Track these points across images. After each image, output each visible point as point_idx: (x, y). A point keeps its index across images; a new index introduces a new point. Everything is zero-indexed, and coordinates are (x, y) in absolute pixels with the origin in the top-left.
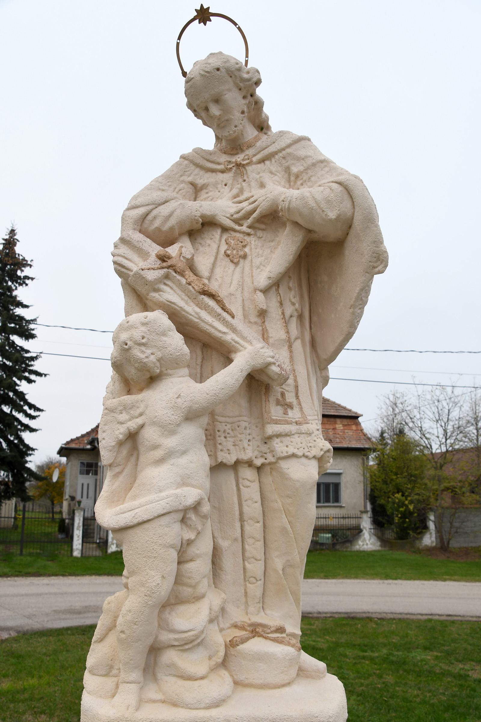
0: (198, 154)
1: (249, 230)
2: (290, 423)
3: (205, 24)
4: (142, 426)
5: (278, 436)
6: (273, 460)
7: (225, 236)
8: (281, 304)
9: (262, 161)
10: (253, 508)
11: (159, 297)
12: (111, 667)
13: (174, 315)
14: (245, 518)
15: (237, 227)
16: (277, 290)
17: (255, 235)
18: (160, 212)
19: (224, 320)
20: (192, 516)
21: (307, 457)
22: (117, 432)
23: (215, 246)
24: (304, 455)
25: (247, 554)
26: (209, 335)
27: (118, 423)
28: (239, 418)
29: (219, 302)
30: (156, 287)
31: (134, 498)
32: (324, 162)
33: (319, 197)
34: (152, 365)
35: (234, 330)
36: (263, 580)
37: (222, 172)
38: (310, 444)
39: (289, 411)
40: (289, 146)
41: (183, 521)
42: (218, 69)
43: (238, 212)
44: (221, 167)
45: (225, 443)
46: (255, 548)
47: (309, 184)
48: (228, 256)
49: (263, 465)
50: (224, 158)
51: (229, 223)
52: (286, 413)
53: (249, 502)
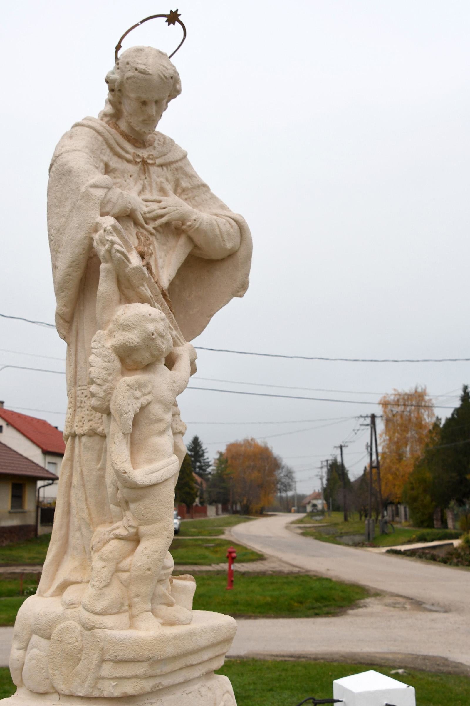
0: (111, 135)
1: (154, 231)
3: (169, 25)
4: (149, 403)
9: (161, 166)
12: (122, 604)
18: (111, 198)
19: (172, 318)
22: (135, 406)
27: (135, 398)
31: (150, 461)
32: (204, 186)
33: (223, 229)
37: (128, 161)
43: (149, 212)
47: (193, 202)
50: (128, 146)
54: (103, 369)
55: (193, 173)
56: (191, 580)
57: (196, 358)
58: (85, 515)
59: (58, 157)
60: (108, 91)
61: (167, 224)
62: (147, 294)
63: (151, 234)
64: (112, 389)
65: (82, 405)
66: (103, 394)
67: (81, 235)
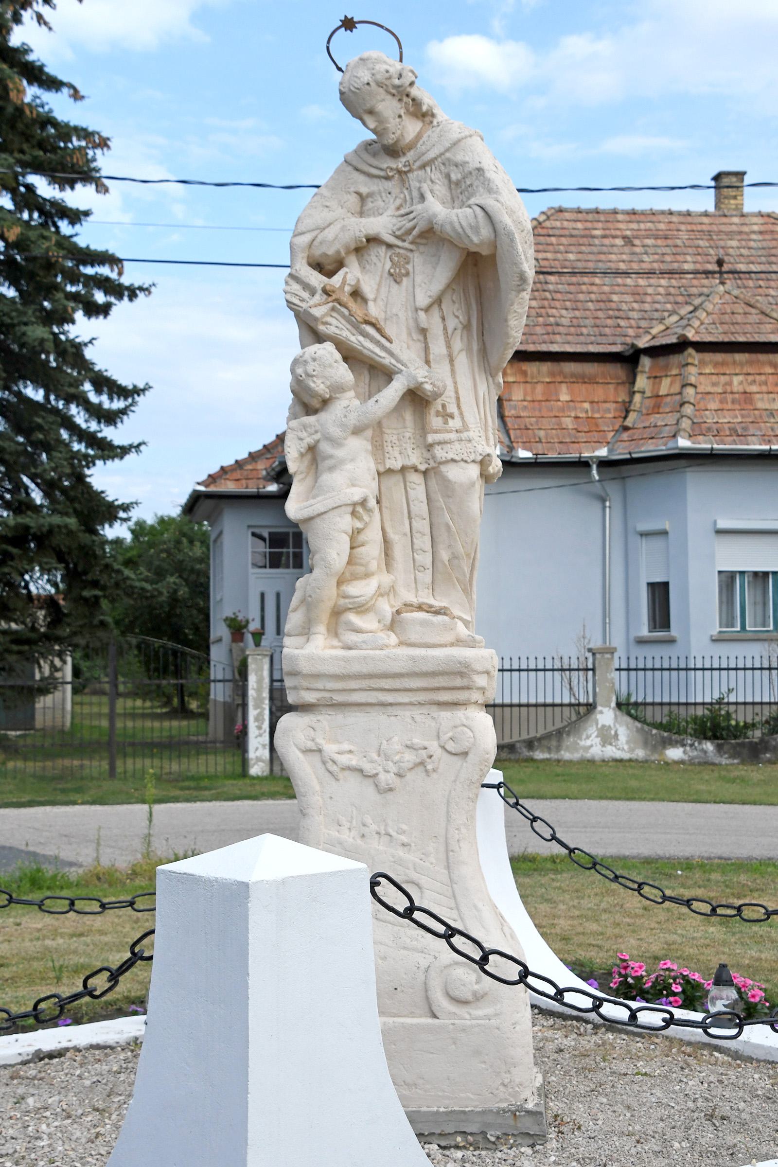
2: (451, 431)
4: (318, 441)
5: (439, 443)
6: (436, 465)
7: (389, 254)
8: (443, 319)
9: (423, 167)
10: (421, 507)
13: (340, 345)
14: (413, 515)
15: (400, 243)
16: (440, 306)
17: (418, 249)
20: (359, 509)
21: (466, 461)
23: (380, 265)
24: (462, 460)
25: (416, 547)
26: (372, 359)
28: (404, 430)
29: (379, 330)
30: (324, 320)
34: (322, 392)
35: (391, 354)
36: (431, 569)
38: (469, 451)
39: (450, 420)
40: (447, 150)
41: (354, 514)
42: (368, 84)
43: (399, 229)
44: (382, 173)
45: (391, 452)
46: (424, 542)
48: (391, 275)
49: (427, 469)
52: (446, 423)
53: (416, 502)
61: (423, 235)
63: (411, 251)
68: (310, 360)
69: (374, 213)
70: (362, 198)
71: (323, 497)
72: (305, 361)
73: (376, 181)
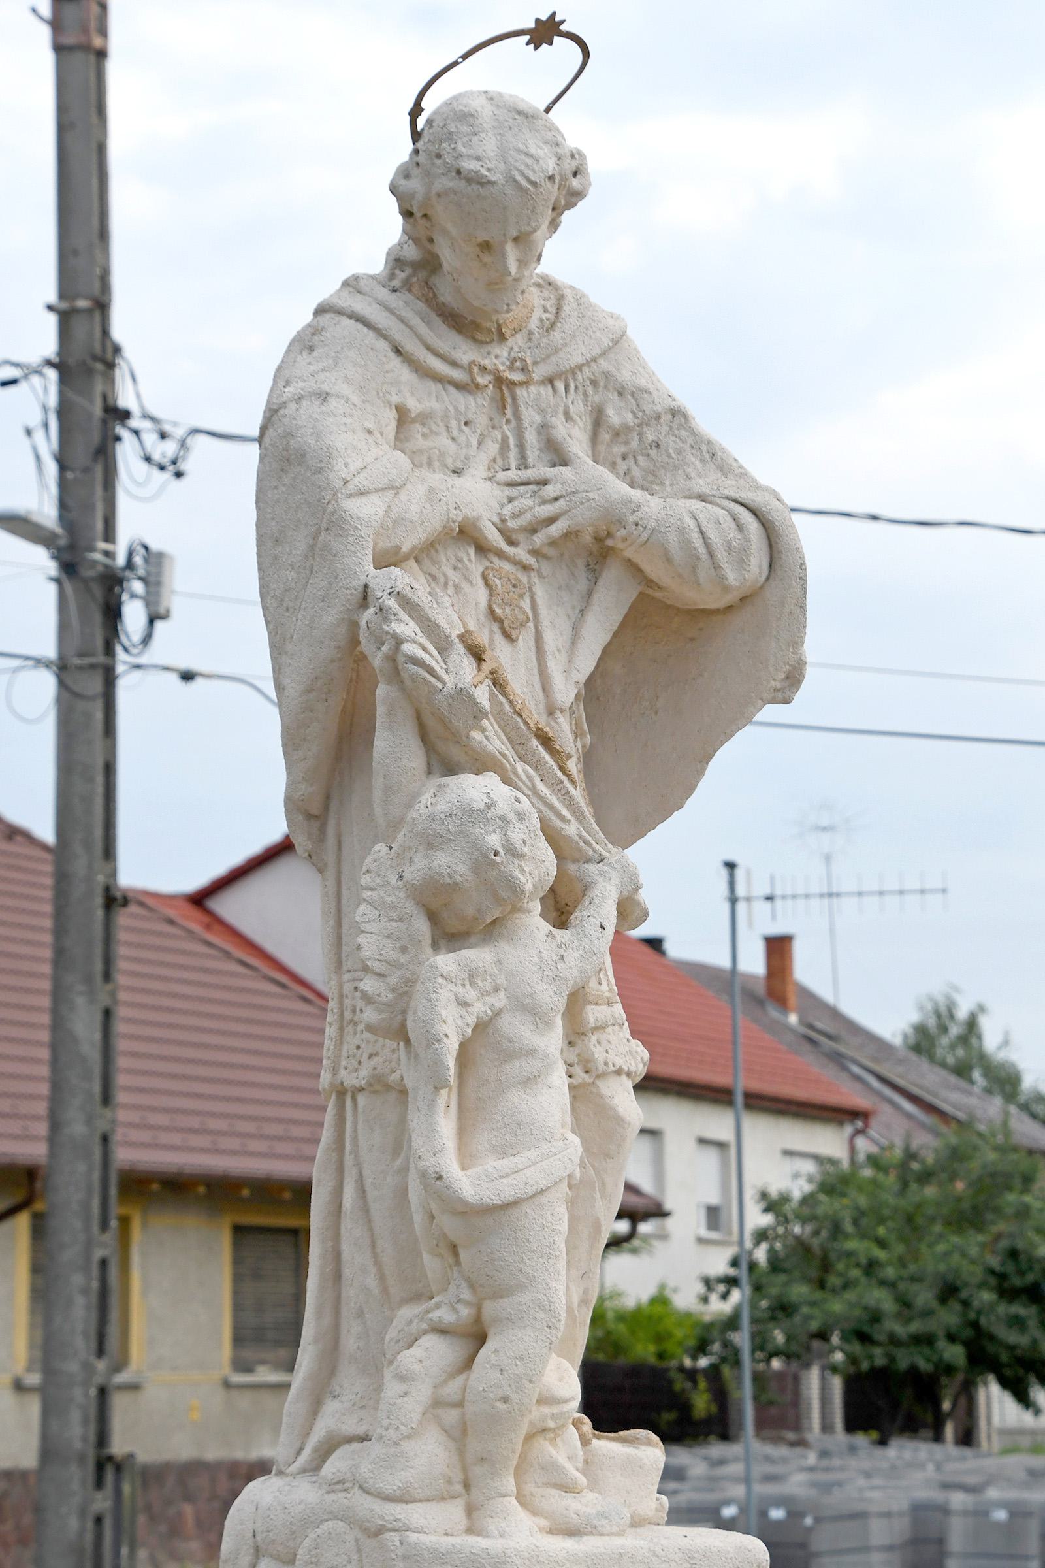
1: (531, 560)
3: (536, 48)
4: (498, 1014)
6: (588, 1079)
11: (485, 742)
19: (568, 792)
27: (459, 1004)
31: (502, 1151)
32: (677, 413)
37: (458, 386)
40: (604, 354)
43: (515, 516)
51: (494, 537)
54: (388, 937)
55: (643, 382)
56: (649, 1443)
57: (637, 888)
58: (372, 1282)
59: (276, 411)
60: (401, 217)
62: (491, 748)
63: (526, 568)
64: (410, 982)
65: (356, 1018)
66: (391, 996)
67: (331, 617)
68: (512, 816)
69: (430, 464)
70: (403, 416)
71: (531, 1154)
72: (503, 818)
73: (434, 387)
